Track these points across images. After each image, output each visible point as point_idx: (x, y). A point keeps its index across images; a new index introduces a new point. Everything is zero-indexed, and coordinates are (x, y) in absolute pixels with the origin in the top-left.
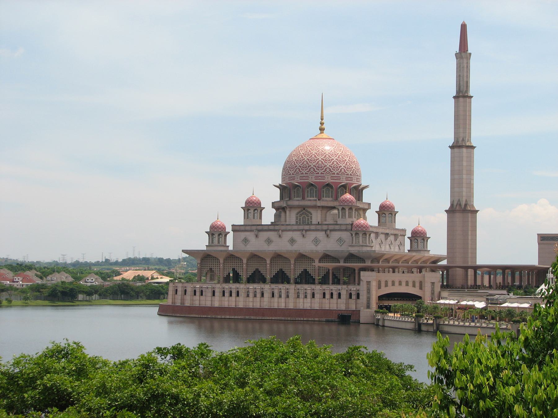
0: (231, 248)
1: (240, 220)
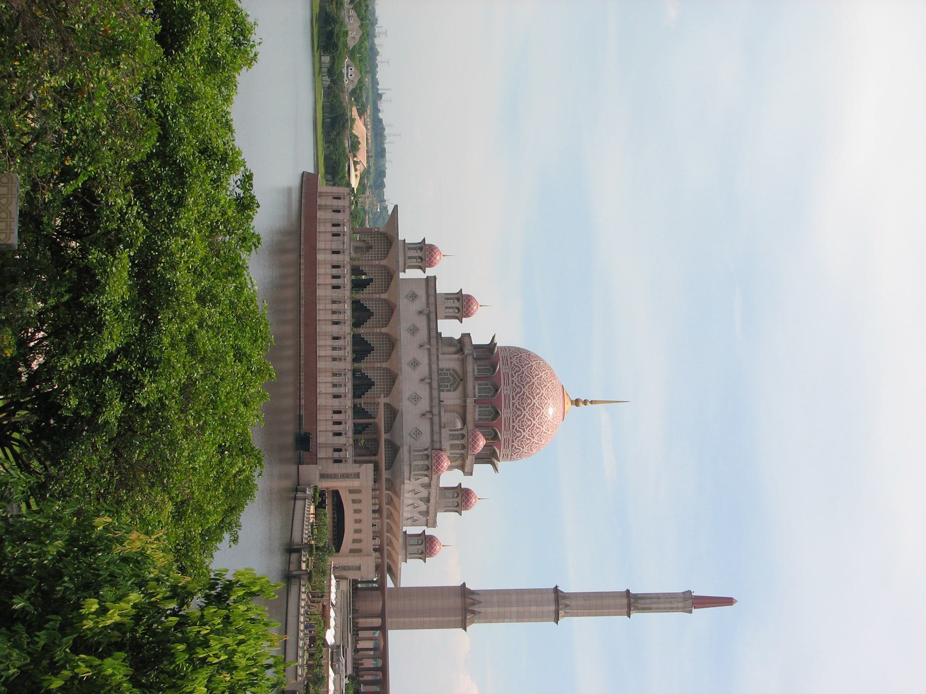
0: (402, 275)
1: (443, 288)
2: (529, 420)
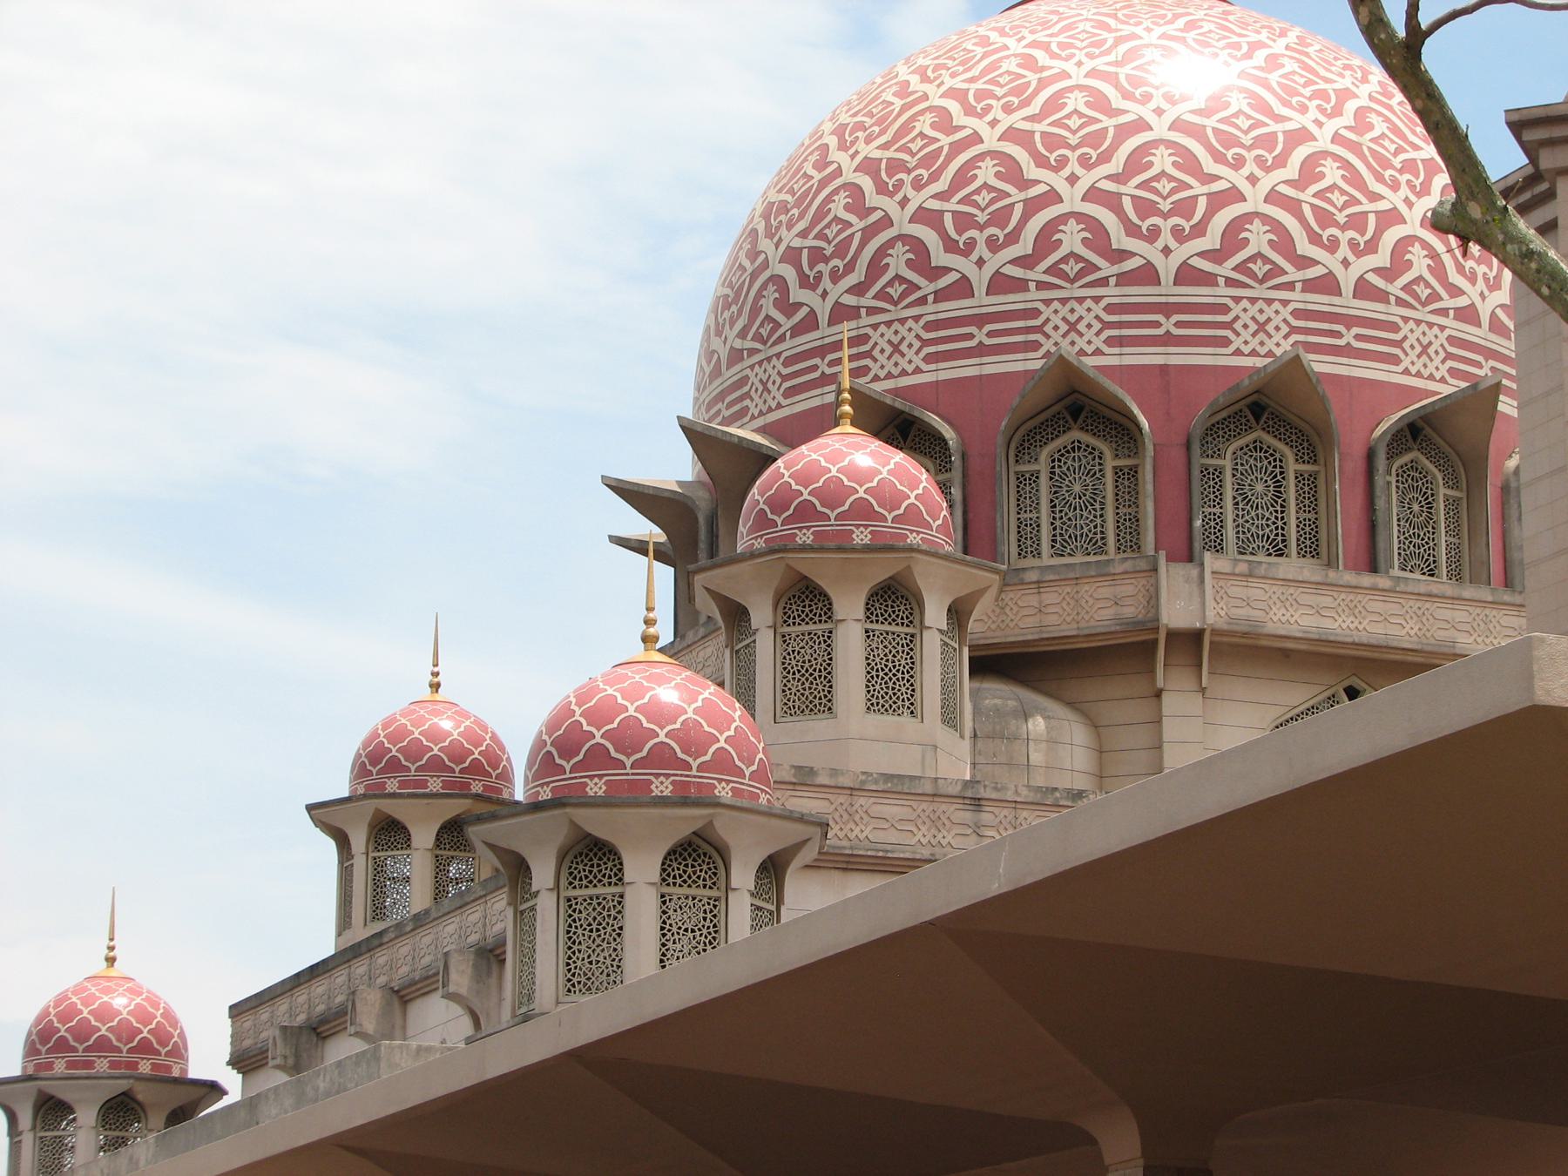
2: (1136, 163)
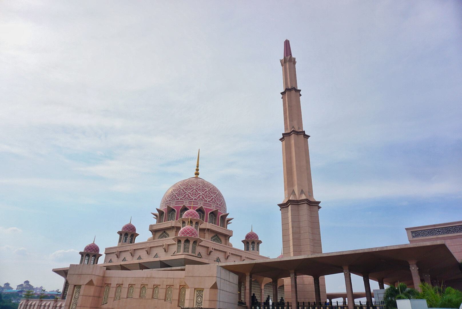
2: (192, 191)
